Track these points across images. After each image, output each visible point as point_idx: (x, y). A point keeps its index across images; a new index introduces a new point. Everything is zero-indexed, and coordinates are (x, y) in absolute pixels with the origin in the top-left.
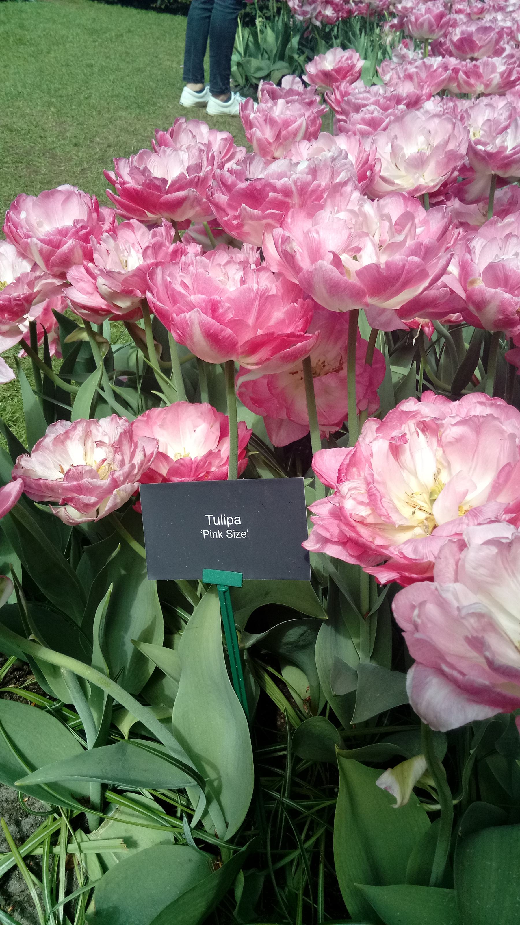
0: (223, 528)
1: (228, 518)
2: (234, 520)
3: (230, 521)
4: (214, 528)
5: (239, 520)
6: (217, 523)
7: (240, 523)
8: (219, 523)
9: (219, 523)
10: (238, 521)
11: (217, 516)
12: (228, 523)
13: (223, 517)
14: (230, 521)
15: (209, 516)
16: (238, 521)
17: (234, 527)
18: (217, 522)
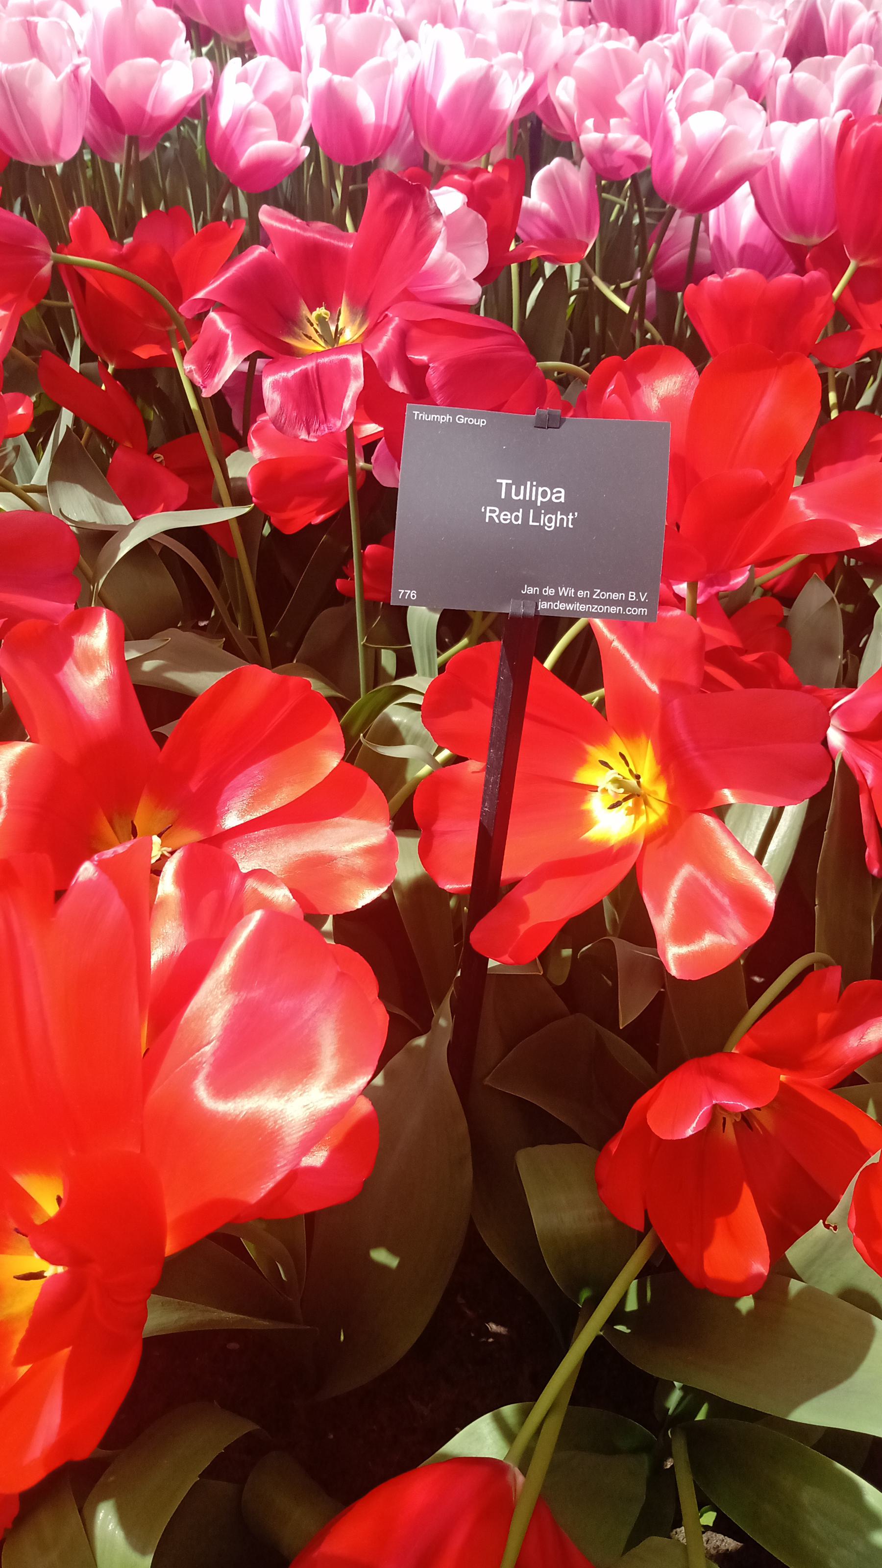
0: (527, 505)
1: (540, 489)
2: (552, 494)
3: (544, 494)
4: (509, 505)
5: (563, 495)
6: (517, 494)
7: (562, 500)
8: (521, 497)
9: (521, 497)
10: (560, 495)
11: (519, 482)
12: (540, 499)
13: (532, 486)
14: (544, 494)
18: (517, 494)
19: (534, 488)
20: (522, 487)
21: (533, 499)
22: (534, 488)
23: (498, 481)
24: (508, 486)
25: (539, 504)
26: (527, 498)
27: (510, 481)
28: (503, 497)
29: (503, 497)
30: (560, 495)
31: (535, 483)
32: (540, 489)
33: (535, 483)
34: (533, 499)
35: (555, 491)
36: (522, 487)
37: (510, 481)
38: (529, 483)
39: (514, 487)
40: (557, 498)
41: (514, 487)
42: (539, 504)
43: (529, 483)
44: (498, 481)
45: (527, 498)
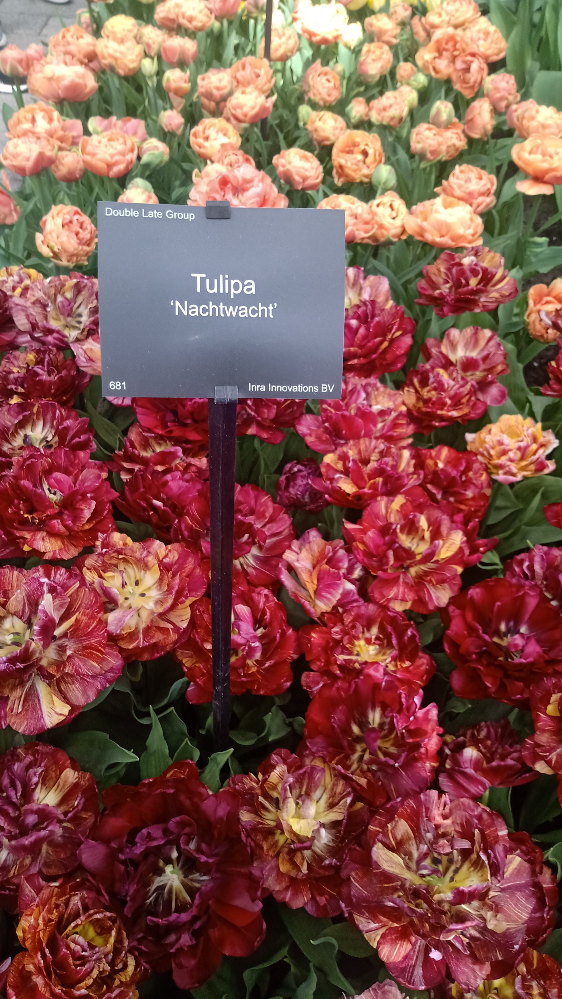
1: (233, 282)
2: (244, 286)
3: (236, 287)
5: (253, 286)
6: (212, 287)
7: (253, 291)
8: (215, 290)
9: (215, 290)
11: (213, 277)
12: (233, 291)
13: (224, 279)
14: (236, 287)
15: (198, 276)
16: (250, 287)
17: (242, 300)
18: (212, 287)
19: (227, 281)
20: (216, 281)
21: (227, 292)
22: (227, 281)
23: (193, 275)
24: (203, 280)
25: (232, 297)
26: (221, 291)
27: (204, 275)
28: (199, 291)
29: (199, 291)
30: (250, 287)
31: (227, 276)
32: (233, 282)
33: (227, 276)
34: (227, 292)
35: (246, 283)
36: (216, 281)
37: (204, 275)
38: (221, 276)
39: (208, 281)
40: (249, 290)
41: (208, 281)
42: (232, 297)
43: (221, 276)
44: (193, 275)
45: (221, 291)
